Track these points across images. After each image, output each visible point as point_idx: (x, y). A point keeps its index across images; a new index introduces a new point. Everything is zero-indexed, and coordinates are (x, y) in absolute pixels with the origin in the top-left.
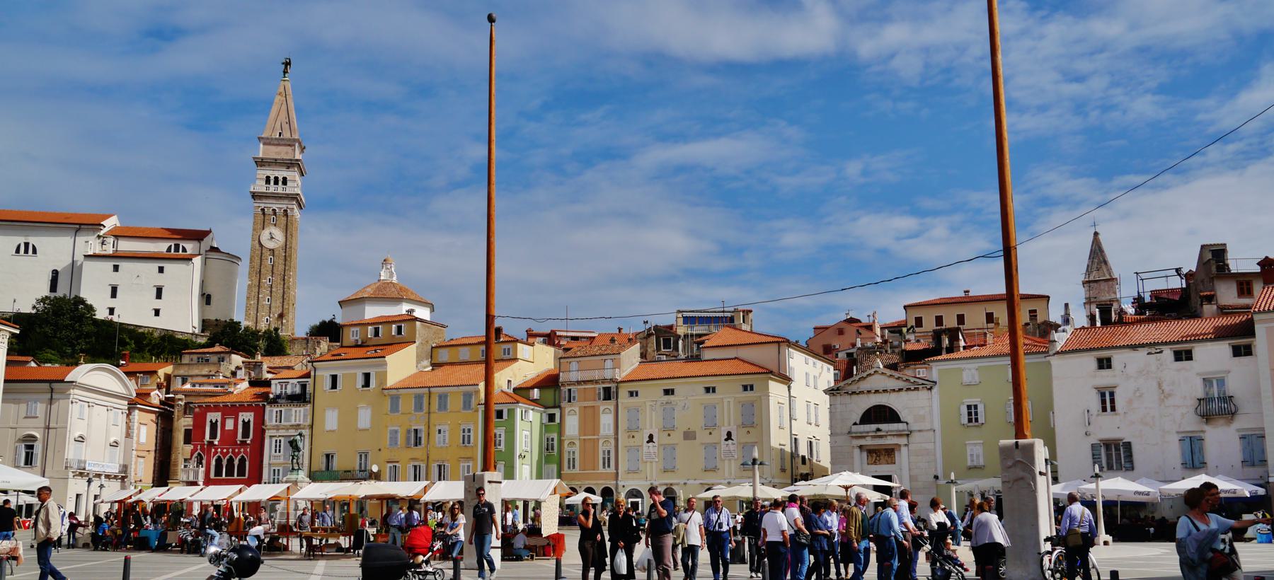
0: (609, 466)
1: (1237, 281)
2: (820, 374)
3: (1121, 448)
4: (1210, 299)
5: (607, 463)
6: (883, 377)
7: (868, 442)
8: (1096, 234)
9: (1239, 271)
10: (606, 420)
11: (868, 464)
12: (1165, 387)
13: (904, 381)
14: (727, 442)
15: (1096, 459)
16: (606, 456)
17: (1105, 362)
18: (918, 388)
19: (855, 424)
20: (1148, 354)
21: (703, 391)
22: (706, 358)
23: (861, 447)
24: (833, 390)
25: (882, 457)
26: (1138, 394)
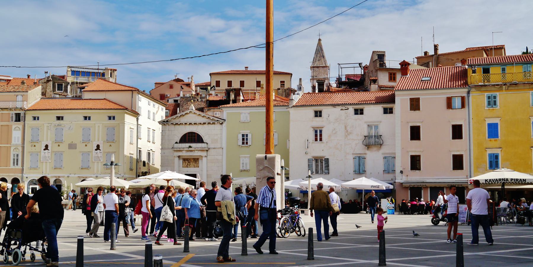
0: (17, 164)
1: (389, 73)
2: (157, 112)
3: (324, 162)
4: (375, 81)
5: (16, 162)
6: (194, 115)
7: (184, 154)
8: (320, 40)
9: (390, 67)
10: (16, 135)
11: (183, 167)
12: (348, 128)
13: (207, 118)
14: (96, 151)
15: (310, 167)
16: (16, 158)
17: (318, 113)
18: (215, 123)
19: (176, 143)
20: (341, 110)
21: (83, 118)
22: (85, 98)
23: (179, 157)
24: (164, 122)
25: (191, 163)
26: (334, 132)
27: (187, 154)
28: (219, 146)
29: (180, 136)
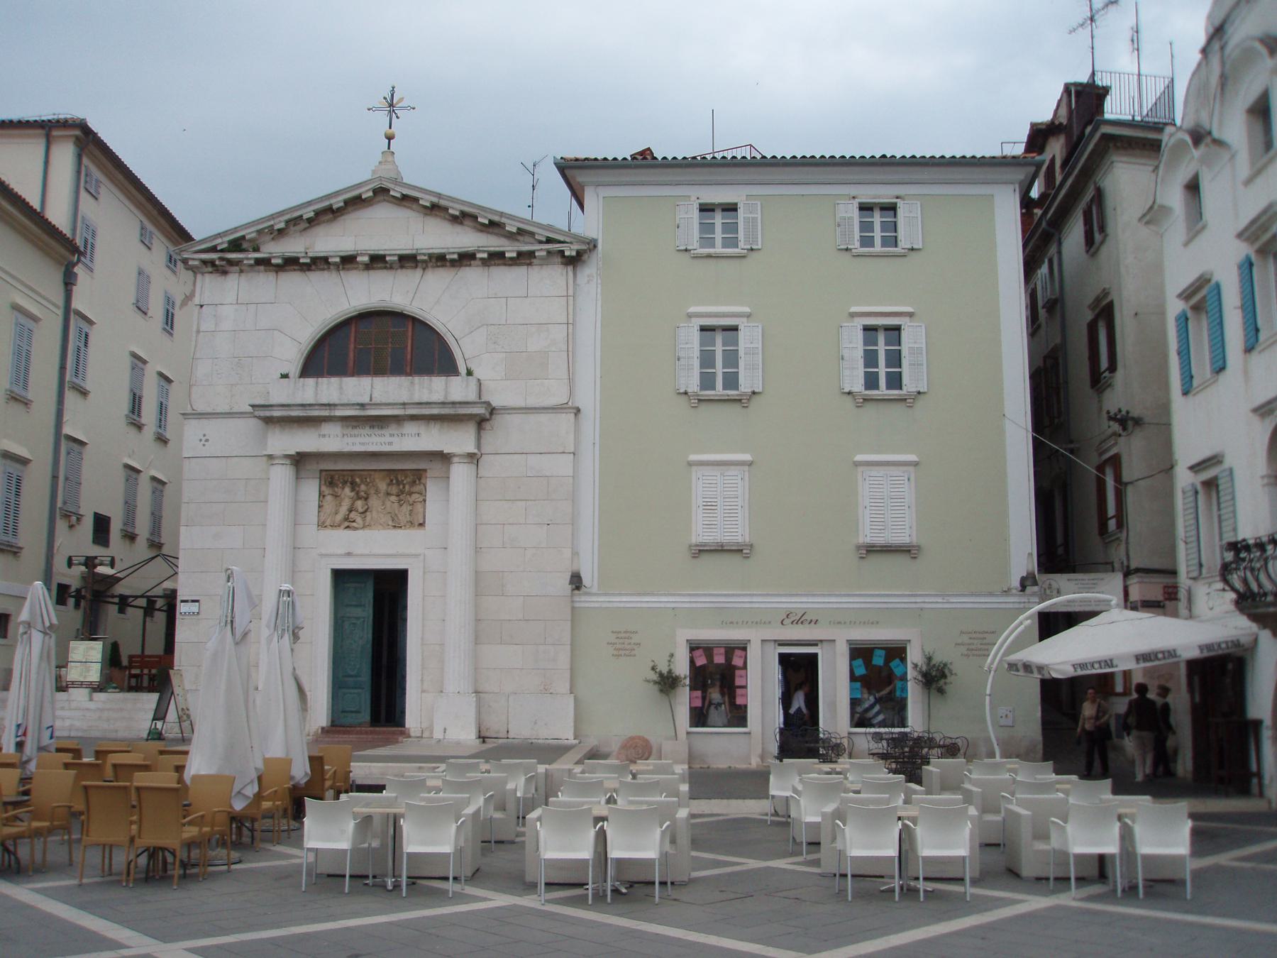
18: (531, 254)
19: (285, 376)
23: (299, 461)
25: (374, 502)
27: (347, 440)
28: (560, 399)
29: (307, 332)
